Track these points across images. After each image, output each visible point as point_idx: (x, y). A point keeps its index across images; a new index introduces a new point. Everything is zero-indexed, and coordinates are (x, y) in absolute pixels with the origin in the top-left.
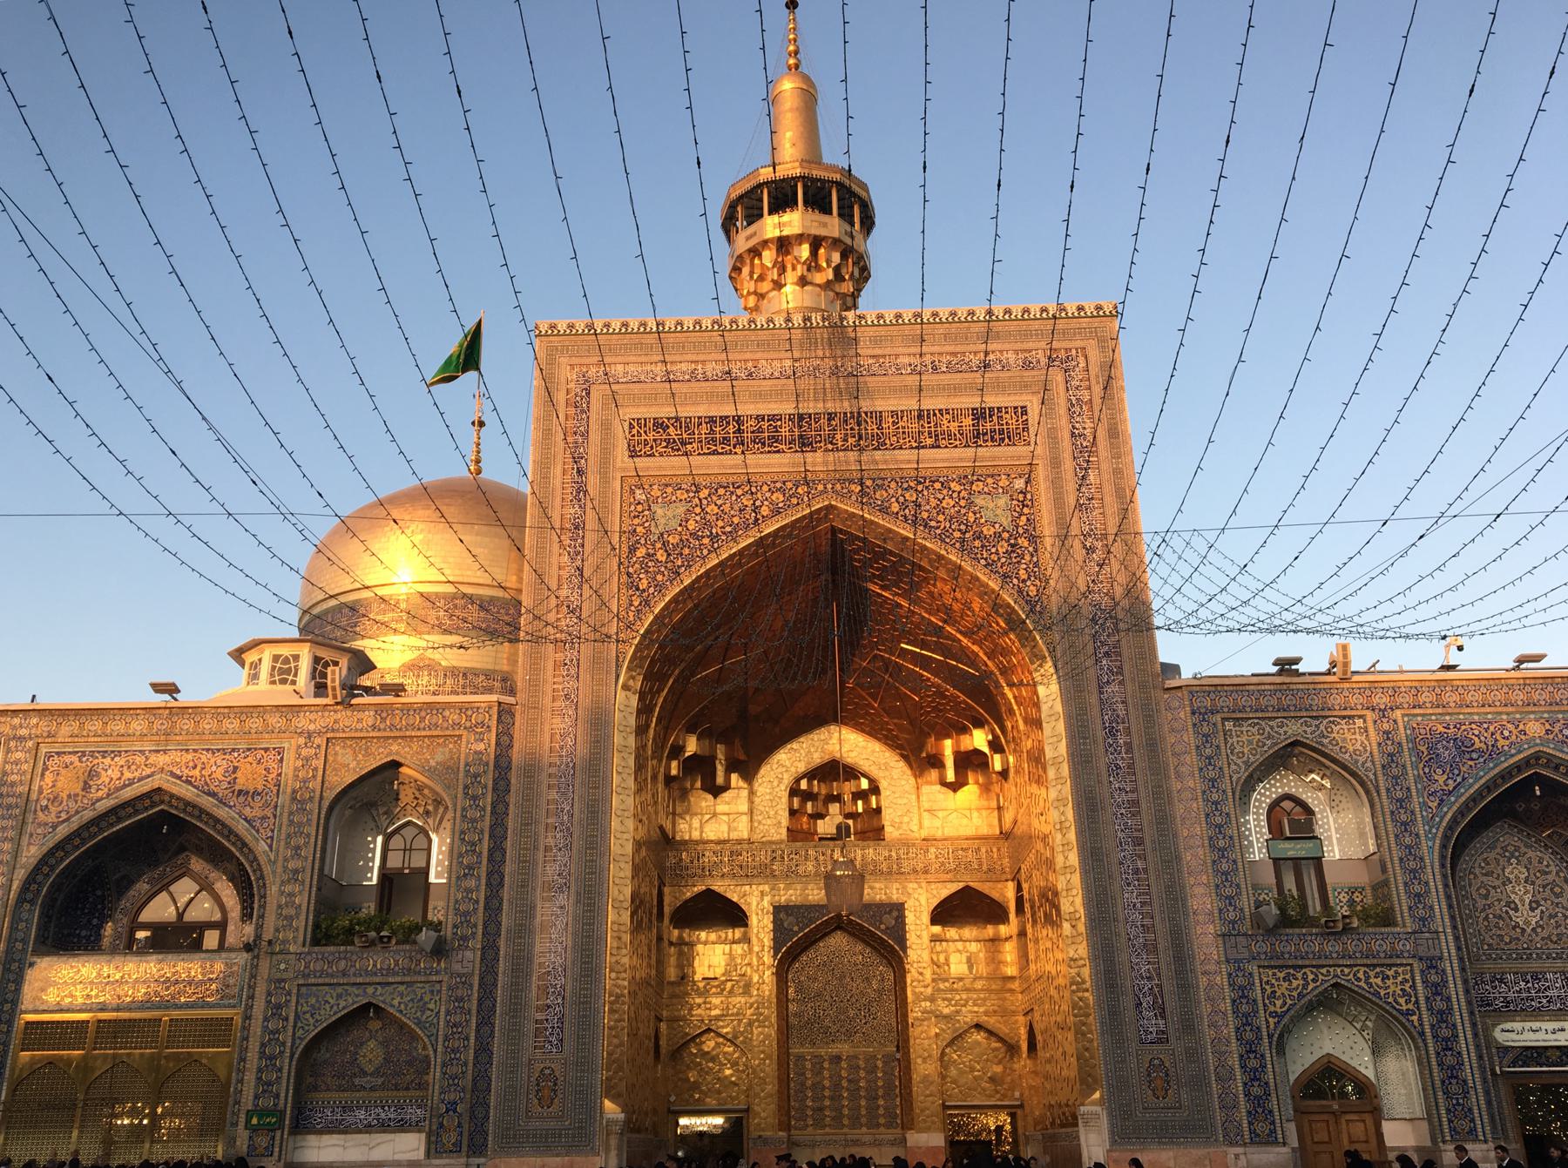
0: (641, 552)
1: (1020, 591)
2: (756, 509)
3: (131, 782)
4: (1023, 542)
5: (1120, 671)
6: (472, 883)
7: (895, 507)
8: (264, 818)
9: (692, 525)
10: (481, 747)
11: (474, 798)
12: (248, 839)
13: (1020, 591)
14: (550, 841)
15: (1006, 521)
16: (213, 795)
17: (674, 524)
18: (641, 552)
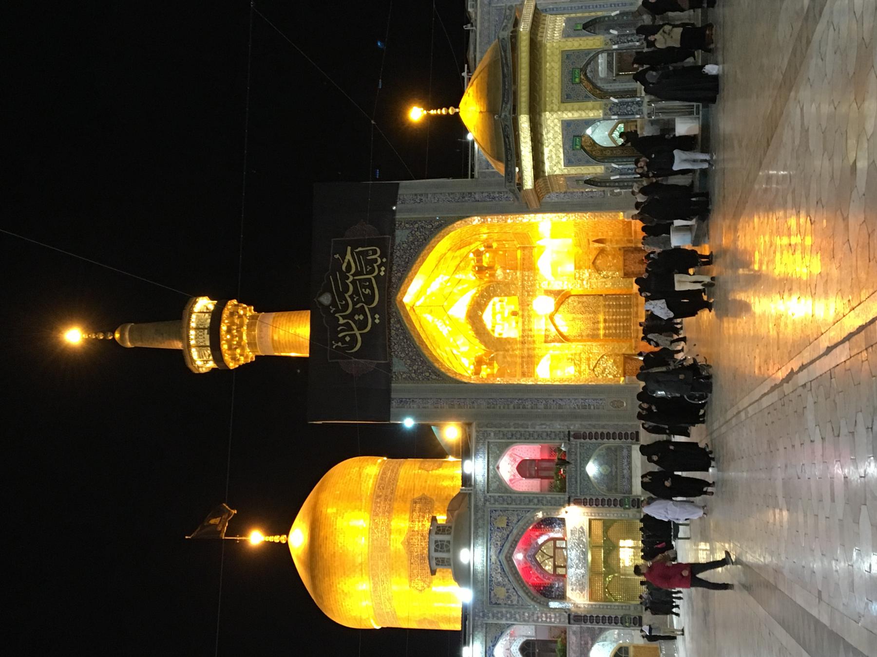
0: (413, 375)
1: (437, 228)
2: (397, 329)
3: (503, 569)
4: (416, 226)
5: (470, 193)
6: (545, 434)
7: (399, 274)
8: (518, 515)
9: (403, 355)
10: (492, 434)
11: (512, 435)
12: (526, 520)
13: (437, 228)
14: (529, 406)
15: (408, 232)
16: (508, 535)
17: (402, 362)
18: (413, 375)
